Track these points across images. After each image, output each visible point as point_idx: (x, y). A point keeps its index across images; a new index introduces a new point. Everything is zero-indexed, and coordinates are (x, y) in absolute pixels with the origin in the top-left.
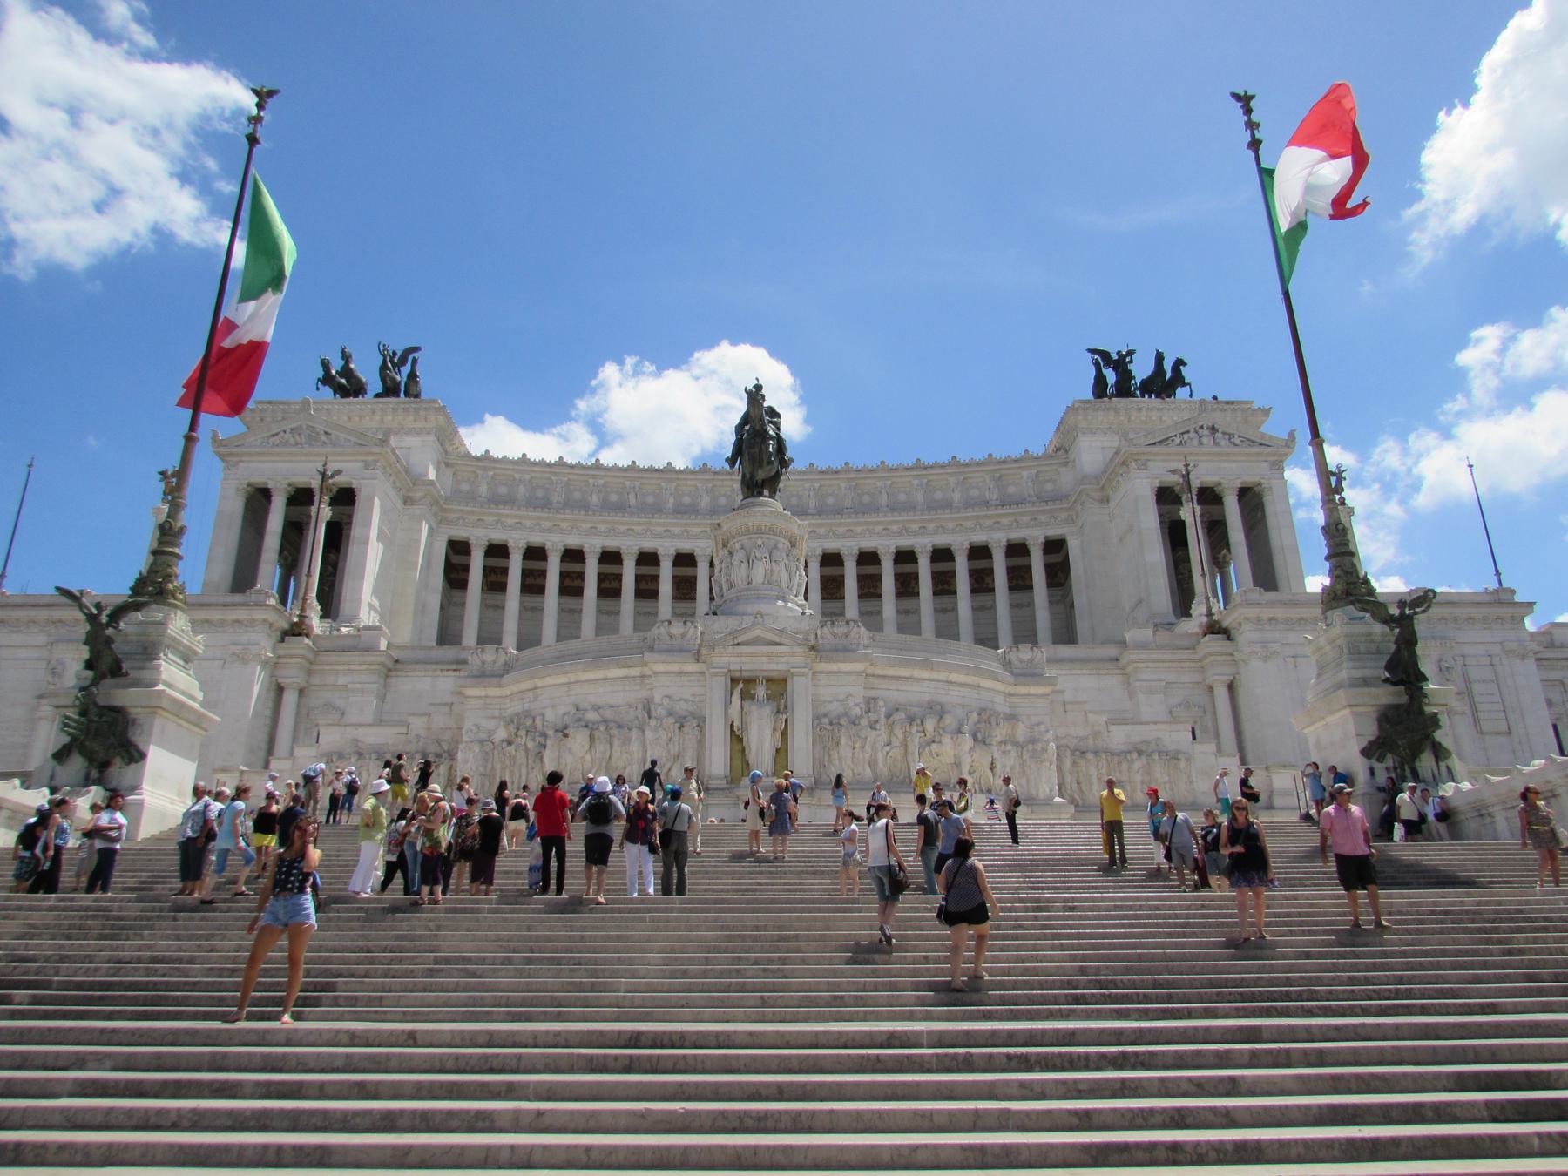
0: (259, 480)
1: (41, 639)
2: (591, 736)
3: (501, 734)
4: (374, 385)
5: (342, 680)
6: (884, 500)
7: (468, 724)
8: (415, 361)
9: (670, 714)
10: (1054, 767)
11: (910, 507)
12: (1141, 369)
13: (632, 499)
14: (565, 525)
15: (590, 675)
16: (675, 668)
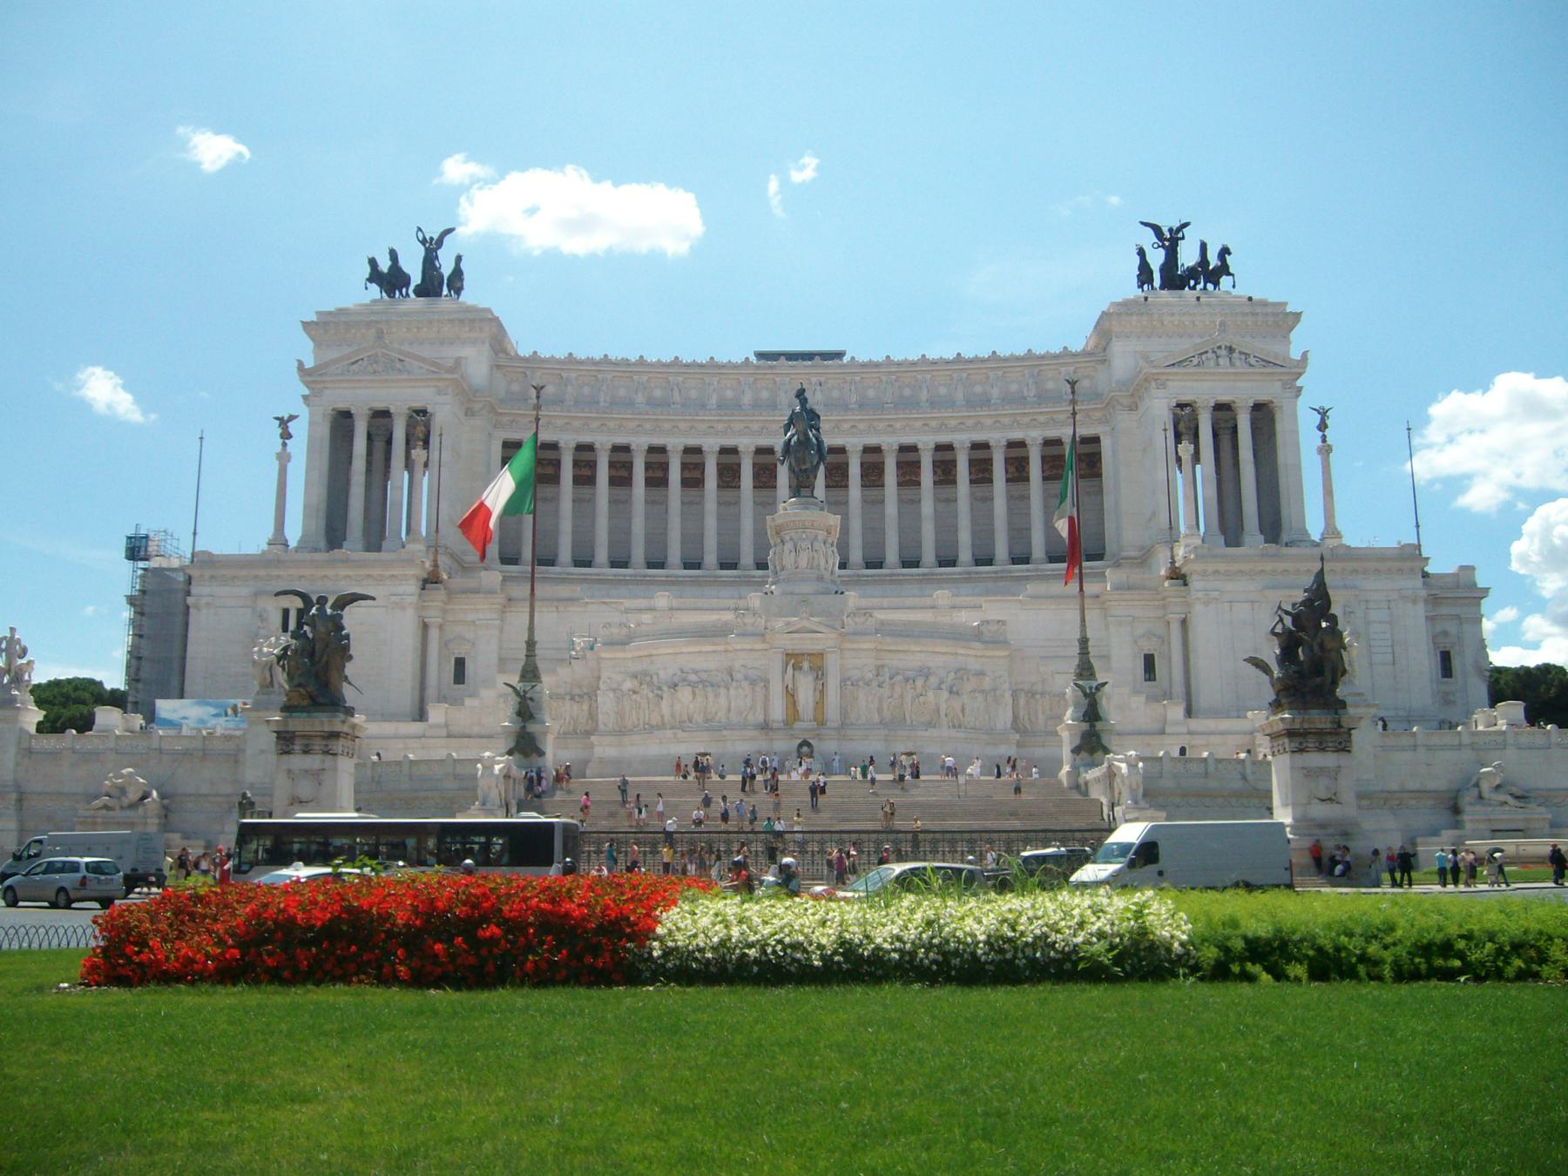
0: (342, 406)
1: (245, 591)
2: (694, 693)
3: (628, 685)
4: (416, 279)
5: (471, 617)
6: (924, 395)
7: (604, 675)
8: (459, 259)
9: (746, 678)
10: (1010, 707)
11: (950, 403)
12: (1188, 256)
13: (677, 397)
14: (611, 424)
15: (691, 649)
16: (748, 647)
